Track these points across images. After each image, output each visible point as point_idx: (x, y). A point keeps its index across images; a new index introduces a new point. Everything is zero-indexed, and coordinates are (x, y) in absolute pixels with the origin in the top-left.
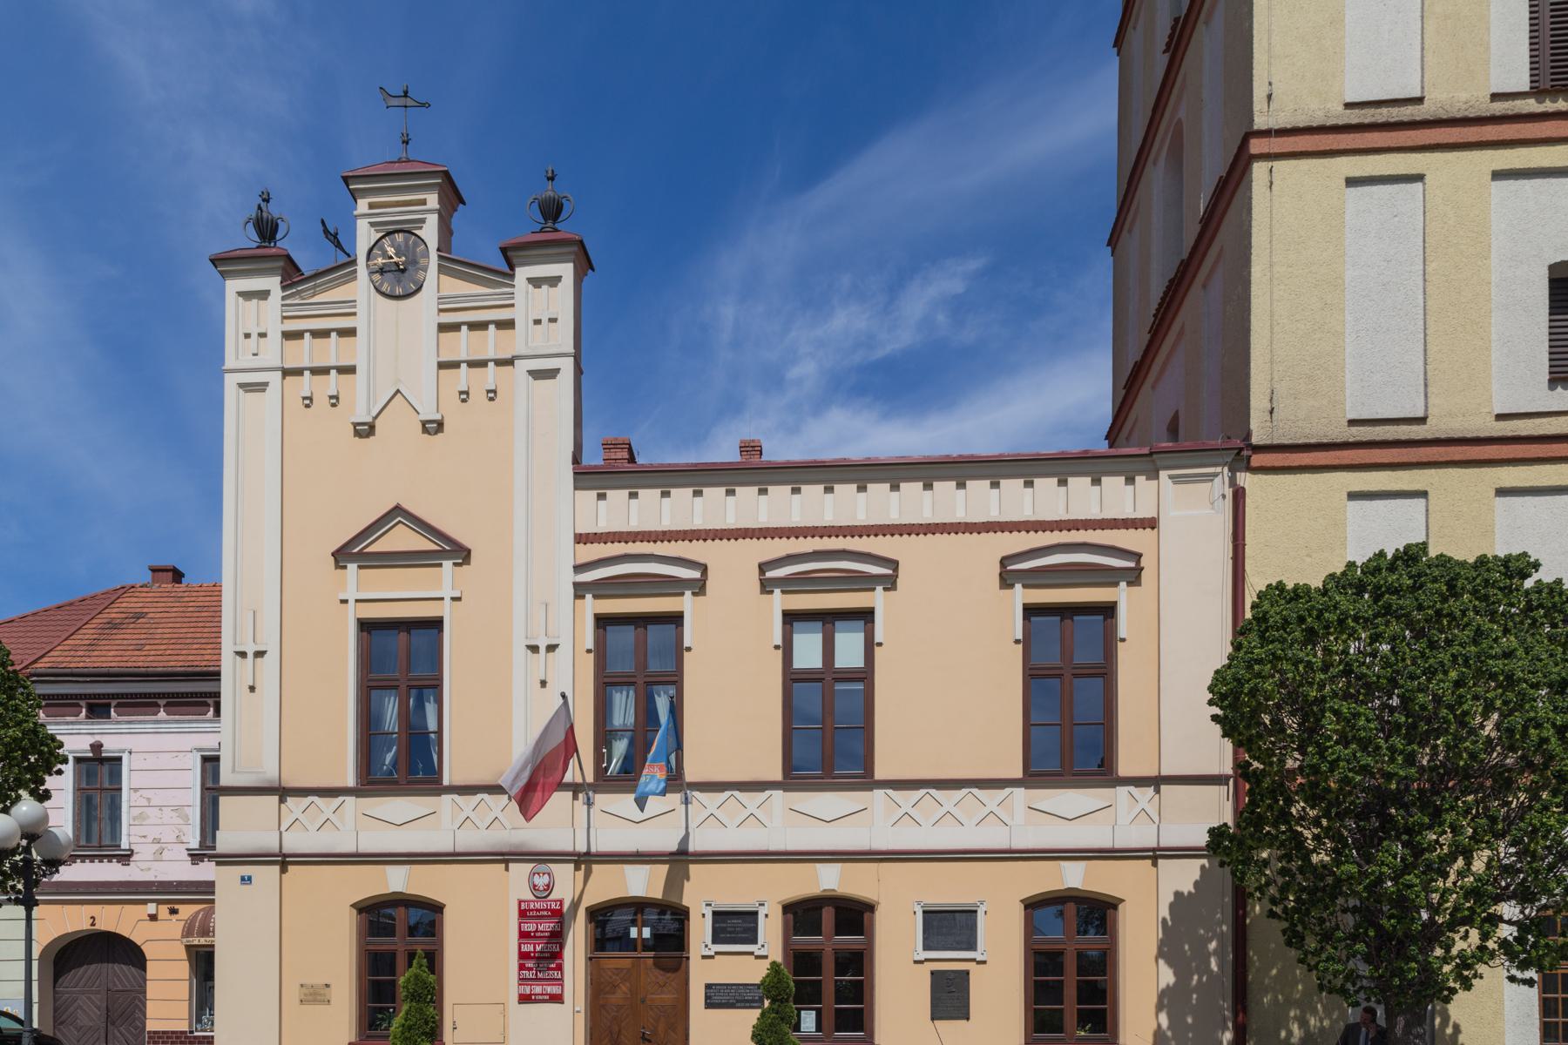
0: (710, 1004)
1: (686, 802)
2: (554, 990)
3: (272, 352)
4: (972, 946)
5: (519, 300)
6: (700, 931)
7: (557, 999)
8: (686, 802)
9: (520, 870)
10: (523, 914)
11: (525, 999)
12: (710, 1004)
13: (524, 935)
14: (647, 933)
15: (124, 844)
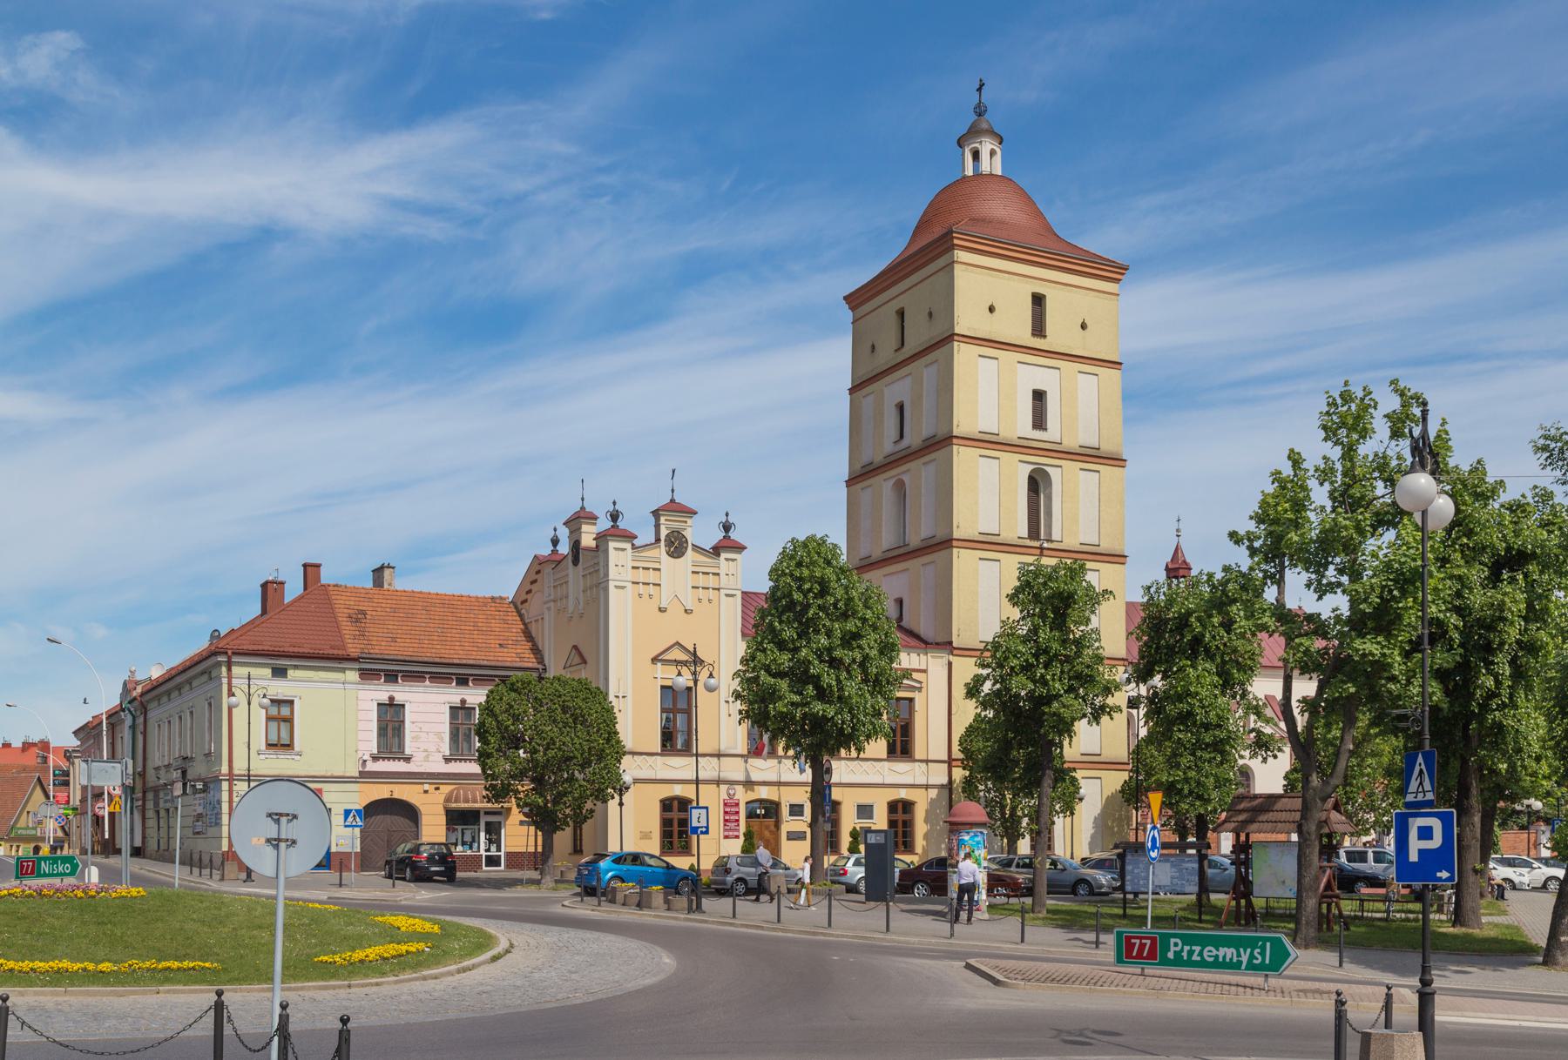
0: (788, 839)
1: (780, 762)
2: (736, 833)
3: (630, 575)
4: (871, 818)
5: (722, 565)
6: (785, 811)
7: (737, 837)
8: (780, 762)
9: (724, 788)
10: (725, 804)
11: (726, 837)
12: (788, 839)
13: (726, 813)
14: (763, 812)
15: (408, 751)
